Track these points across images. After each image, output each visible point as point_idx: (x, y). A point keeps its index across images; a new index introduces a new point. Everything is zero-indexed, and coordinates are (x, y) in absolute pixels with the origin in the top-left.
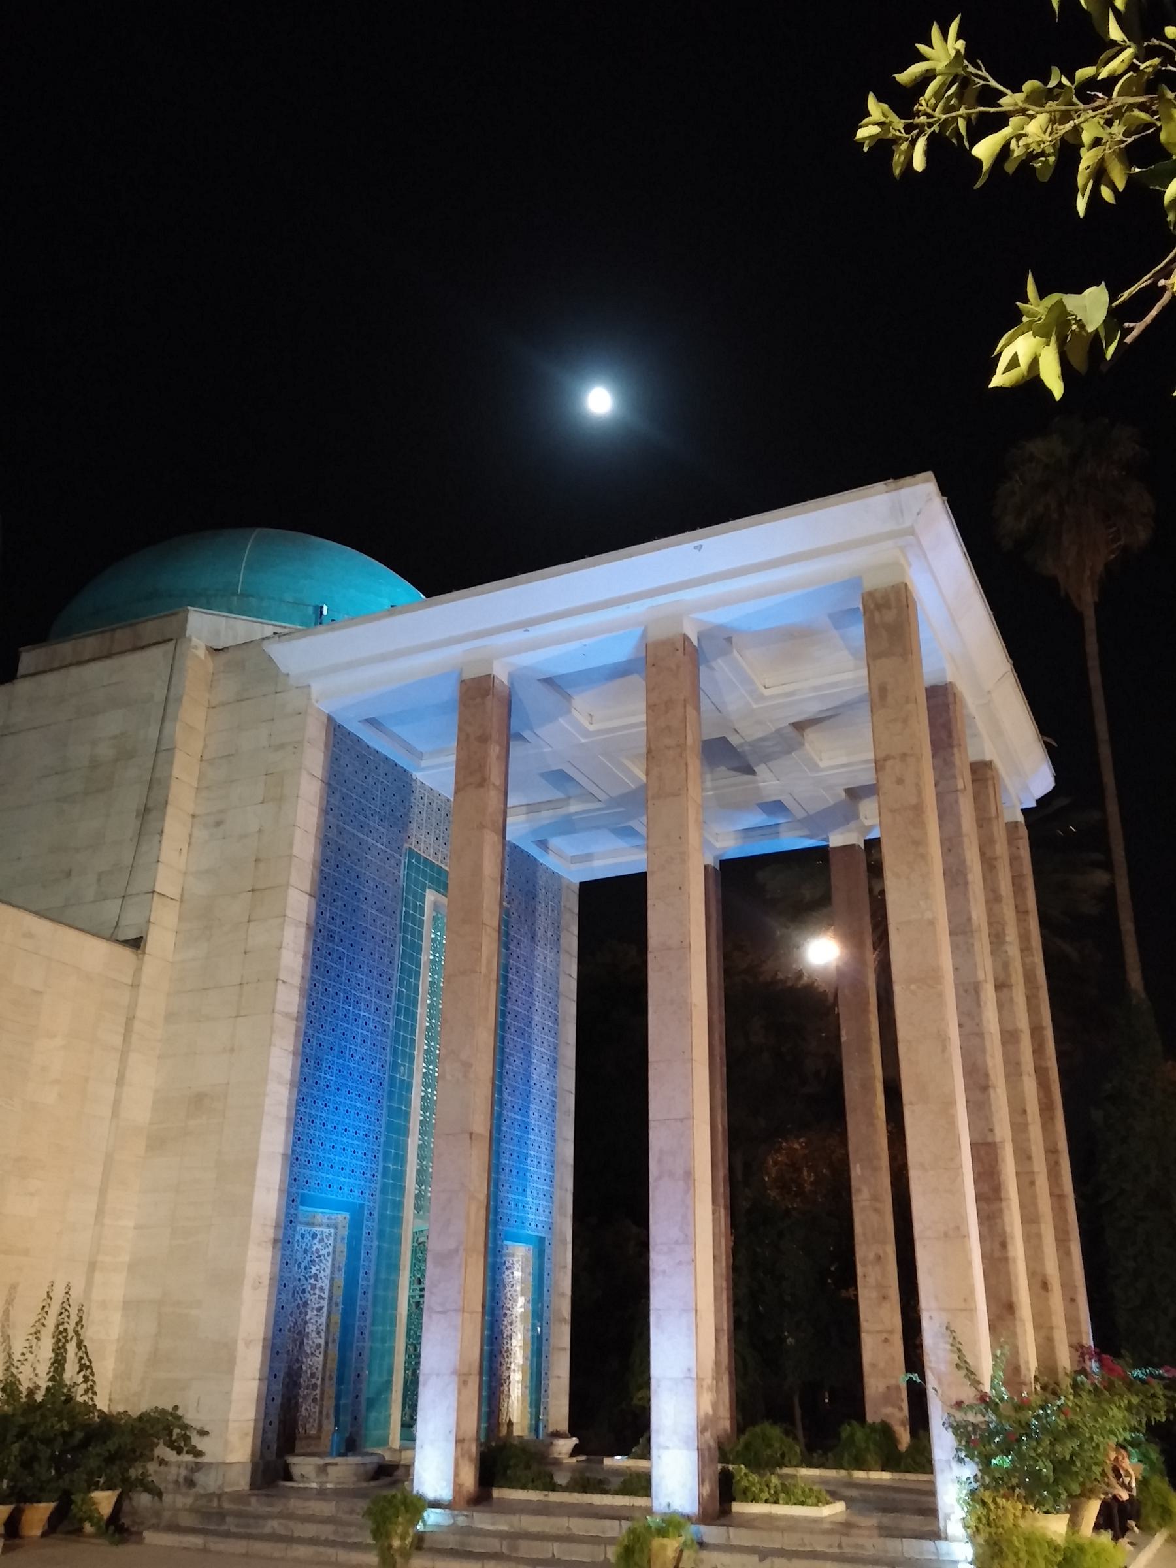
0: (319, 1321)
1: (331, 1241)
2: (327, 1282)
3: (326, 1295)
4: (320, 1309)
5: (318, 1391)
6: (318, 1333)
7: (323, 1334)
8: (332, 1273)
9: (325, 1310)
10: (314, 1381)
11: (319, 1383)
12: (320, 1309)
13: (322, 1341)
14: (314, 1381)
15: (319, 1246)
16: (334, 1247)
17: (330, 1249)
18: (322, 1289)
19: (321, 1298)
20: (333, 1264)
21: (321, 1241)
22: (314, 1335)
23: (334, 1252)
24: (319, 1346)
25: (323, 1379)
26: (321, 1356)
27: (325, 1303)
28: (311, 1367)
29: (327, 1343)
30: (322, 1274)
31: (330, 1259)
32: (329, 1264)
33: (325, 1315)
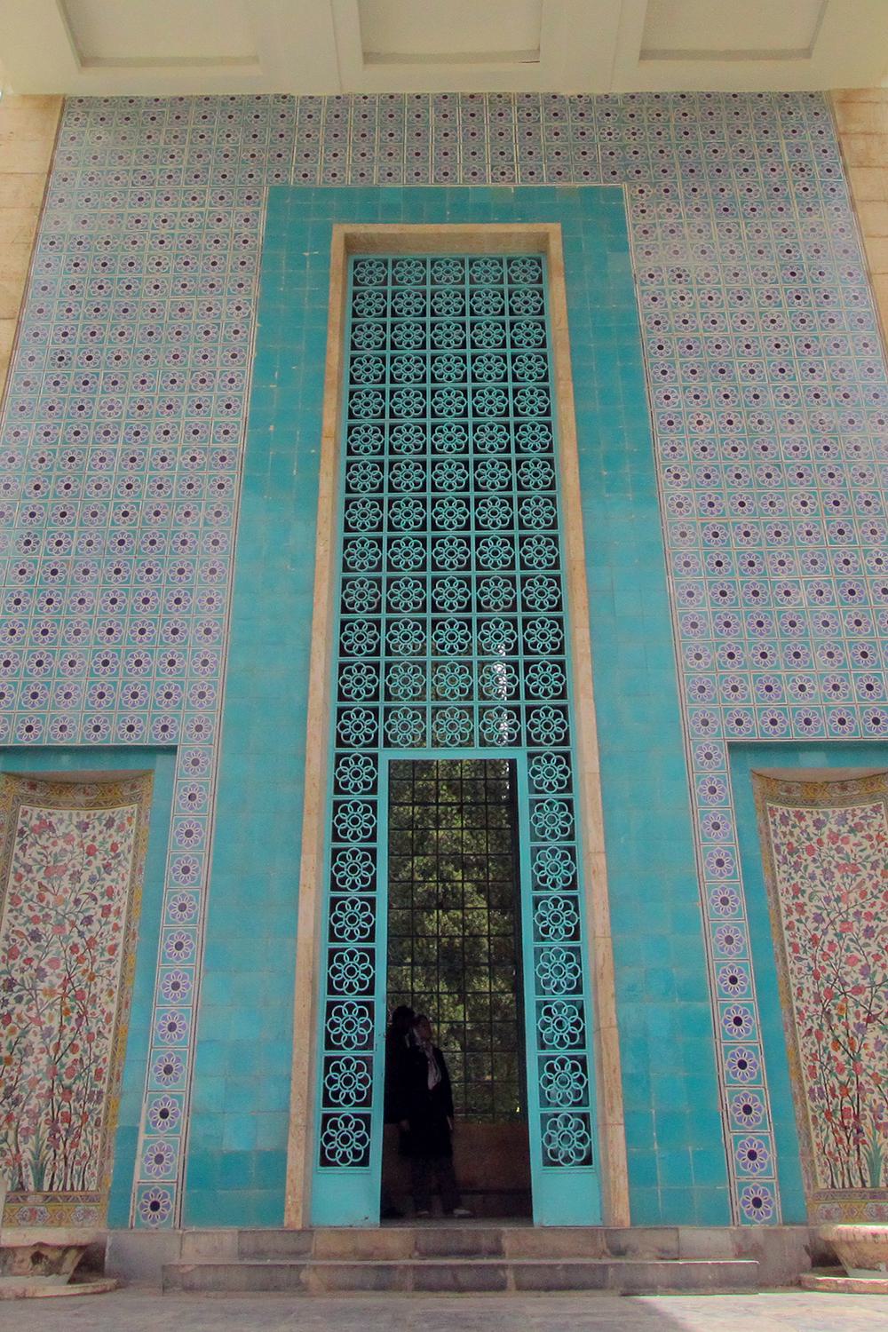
0: (113, 974)
1: (133, 827)
2: (125, 898)
3: (122, 923)
4: (112, 950)
5: (103, 1105)
6: (111, 993)
7: (116, 995)
8: (132, 881)
9: (120, 949)
11: (105, 1088)
12: (112, 950)
13: (113, 1008)
15: (117, 839)
17: (131, 841)
18: (118, 912)
19: (116, 928)
20: (134, 864)
21: (121, 828)
22: (104, 997)
23: (136, 843)
26: (111, 1036)
27: (120, 936)
28: (97, 1058)
31: (130, 857)
32: (129, 867)
33: (120, 959)
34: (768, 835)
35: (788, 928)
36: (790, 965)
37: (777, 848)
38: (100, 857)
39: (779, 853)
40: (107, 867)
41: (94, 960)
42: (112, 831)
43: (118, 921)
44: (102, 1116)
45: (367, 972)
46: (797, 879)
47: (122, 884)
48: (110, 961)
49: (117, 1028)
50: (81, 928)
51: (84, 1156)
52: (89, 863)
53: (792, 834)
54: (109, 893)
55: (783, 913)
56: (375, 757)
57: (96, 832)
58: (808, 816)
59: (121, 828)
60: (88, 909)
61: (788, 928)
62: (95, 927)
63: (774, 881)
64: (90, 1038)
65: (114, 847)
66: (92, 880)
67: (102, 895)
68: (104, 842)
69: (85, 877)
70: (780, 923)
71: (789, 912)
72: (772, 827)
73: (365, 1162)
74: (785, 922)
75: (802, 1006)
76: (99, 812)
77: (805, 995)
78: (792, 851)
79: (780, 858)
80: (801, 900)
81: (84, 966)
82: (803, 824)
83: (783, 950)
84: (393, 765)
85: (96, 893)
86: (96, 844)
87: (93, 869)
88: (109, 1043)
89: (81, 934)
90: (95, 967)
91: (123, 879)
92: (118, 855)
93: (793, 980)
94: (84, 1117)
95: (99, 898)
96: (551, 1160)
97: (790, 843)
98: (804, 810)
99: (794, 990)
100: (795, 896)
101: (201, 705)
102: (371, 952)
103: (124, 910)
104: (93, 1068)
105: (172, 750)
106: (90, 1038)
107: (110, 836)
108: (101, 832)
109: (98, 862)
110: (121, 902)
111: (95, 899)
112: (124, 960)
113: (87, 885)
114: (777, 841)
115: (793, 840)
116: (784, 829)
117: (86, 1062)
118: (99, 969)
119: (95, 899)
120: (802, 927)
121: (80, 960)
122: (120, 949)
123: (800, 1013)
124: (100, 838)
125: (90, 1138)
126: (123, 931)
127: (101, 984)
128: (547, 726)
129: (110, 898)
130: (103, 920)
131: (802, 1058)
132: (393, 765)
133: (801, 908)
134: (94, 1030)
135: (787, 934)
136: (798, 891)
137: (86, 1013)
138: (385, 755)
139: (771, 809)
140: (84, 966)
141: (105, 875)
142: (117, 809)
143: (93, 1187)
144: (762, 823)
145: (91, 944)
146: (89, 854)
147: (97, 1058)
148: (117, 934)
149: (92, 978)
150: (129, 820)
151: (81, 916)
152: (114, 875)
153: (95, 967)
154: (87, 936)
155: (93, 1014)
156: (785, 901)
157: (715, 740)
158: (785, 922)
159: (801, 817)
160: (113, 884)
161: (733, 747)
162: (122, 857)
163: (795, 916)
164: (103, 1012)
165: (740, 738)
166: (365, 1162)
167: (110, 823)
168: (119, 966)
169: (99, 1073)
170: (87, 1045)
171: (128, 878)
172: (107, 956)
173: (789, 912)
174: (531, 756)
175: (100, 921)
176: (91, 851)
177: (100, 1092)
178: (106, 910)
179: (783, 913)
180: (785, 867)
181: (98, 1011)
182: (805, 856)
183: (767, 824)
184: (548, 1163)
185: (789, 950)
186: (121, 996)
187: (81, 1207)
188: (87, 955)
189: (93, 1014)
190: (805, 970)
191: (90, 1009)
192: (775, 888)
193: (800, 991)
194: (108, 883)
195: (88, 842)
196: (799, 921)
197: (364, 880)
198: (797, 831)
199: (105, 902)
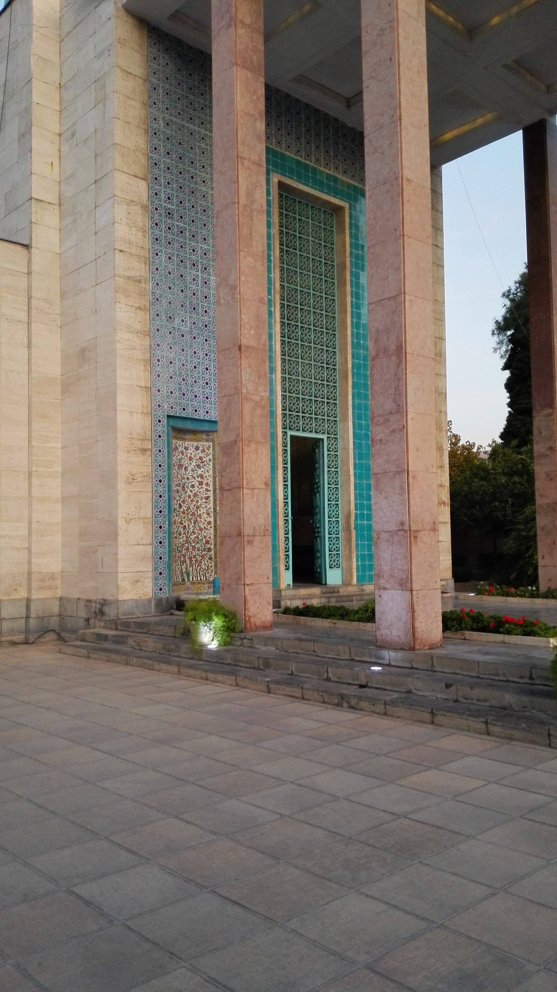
1: (211, 451)
2: (211, 479)
3: (211, 488)
4: (207, 498)
6: (208, 514)
7: (212, 515)
9: (211, 498)
10: (209, 546)
11: (212, 547)
12: (207, 498)
13: (212, 520)
14: (209, 546)
15: (201, 455)
16: (214, 455)
17: (211, 457)
18: (207, 484)
19: (207, 490)
20: (214, 467)
21: (203, 451)
22: (205, 515)
23: (214, 459)
24: (209, 523)
25: (215, 545)
26: (212, 530)
27: (211, 494)
28: (205, 537)
29: (215, 521)
31: (211, 464)
32: (211, 467)
33: (212, 502)
38: (194, 461)
40: (198, 466)
41: (197, 502)
42: (198, 451)
43: (208, 488)
44: (213, 556)
49: (215, 527)
50: (191, 489)
51: (205, 569)
52: (191, 464)
54: (201, 476)
60: (192, 482)
62: (196, 489)
66: (193, 470)
68: (195, 456)
69: (189, 469)
76: (192, 443)
81: (194, 503)
84: (291, 436)
86: (192, 456)
87: (192, 466)
89: (191, 491)
90: (199, 504)
91: (208, 472)
92: (204, 462)
94: (203, 557)
95: (196, 478)
104: (204, 540)
107: (198, 454)
108: (193, 451)
109: (194, 463)
111: (194, 478)
113: (191, 472)
117: (200, 538)
118: (201, 505)
119: (194, 478)
121: (192, 501)
124: (193, 454)
125: (207, 563)
126: (212, 492)
127: (202, 511)
130: (200, 487)
132: (291, 436)
134: (202, 527)
137: (197, 520)
140: (194, 503)
141: (198, 469)
142: (200, 443)
145: (195, 495)
148: (208, 493)
149: (198, 508)
150: (208, 449)
151: (190, 484)
152: (202, 469)
153: (199, 504)
154: (194, 492)
155: (201, 521)
160: (203, 473)
162: (205, 463)
164: (205, 520)
167: (197, 448)
169: (207, 542)
170: (200, 532)
172: (204, 500)
175: (198, 487)
178: (201, 483)
181: (203, 520)
184: (330, 567)
188: (194, 499)
189: (201, 521)
191: (198, 519)
195: (189, 455)
199: (199, 479)
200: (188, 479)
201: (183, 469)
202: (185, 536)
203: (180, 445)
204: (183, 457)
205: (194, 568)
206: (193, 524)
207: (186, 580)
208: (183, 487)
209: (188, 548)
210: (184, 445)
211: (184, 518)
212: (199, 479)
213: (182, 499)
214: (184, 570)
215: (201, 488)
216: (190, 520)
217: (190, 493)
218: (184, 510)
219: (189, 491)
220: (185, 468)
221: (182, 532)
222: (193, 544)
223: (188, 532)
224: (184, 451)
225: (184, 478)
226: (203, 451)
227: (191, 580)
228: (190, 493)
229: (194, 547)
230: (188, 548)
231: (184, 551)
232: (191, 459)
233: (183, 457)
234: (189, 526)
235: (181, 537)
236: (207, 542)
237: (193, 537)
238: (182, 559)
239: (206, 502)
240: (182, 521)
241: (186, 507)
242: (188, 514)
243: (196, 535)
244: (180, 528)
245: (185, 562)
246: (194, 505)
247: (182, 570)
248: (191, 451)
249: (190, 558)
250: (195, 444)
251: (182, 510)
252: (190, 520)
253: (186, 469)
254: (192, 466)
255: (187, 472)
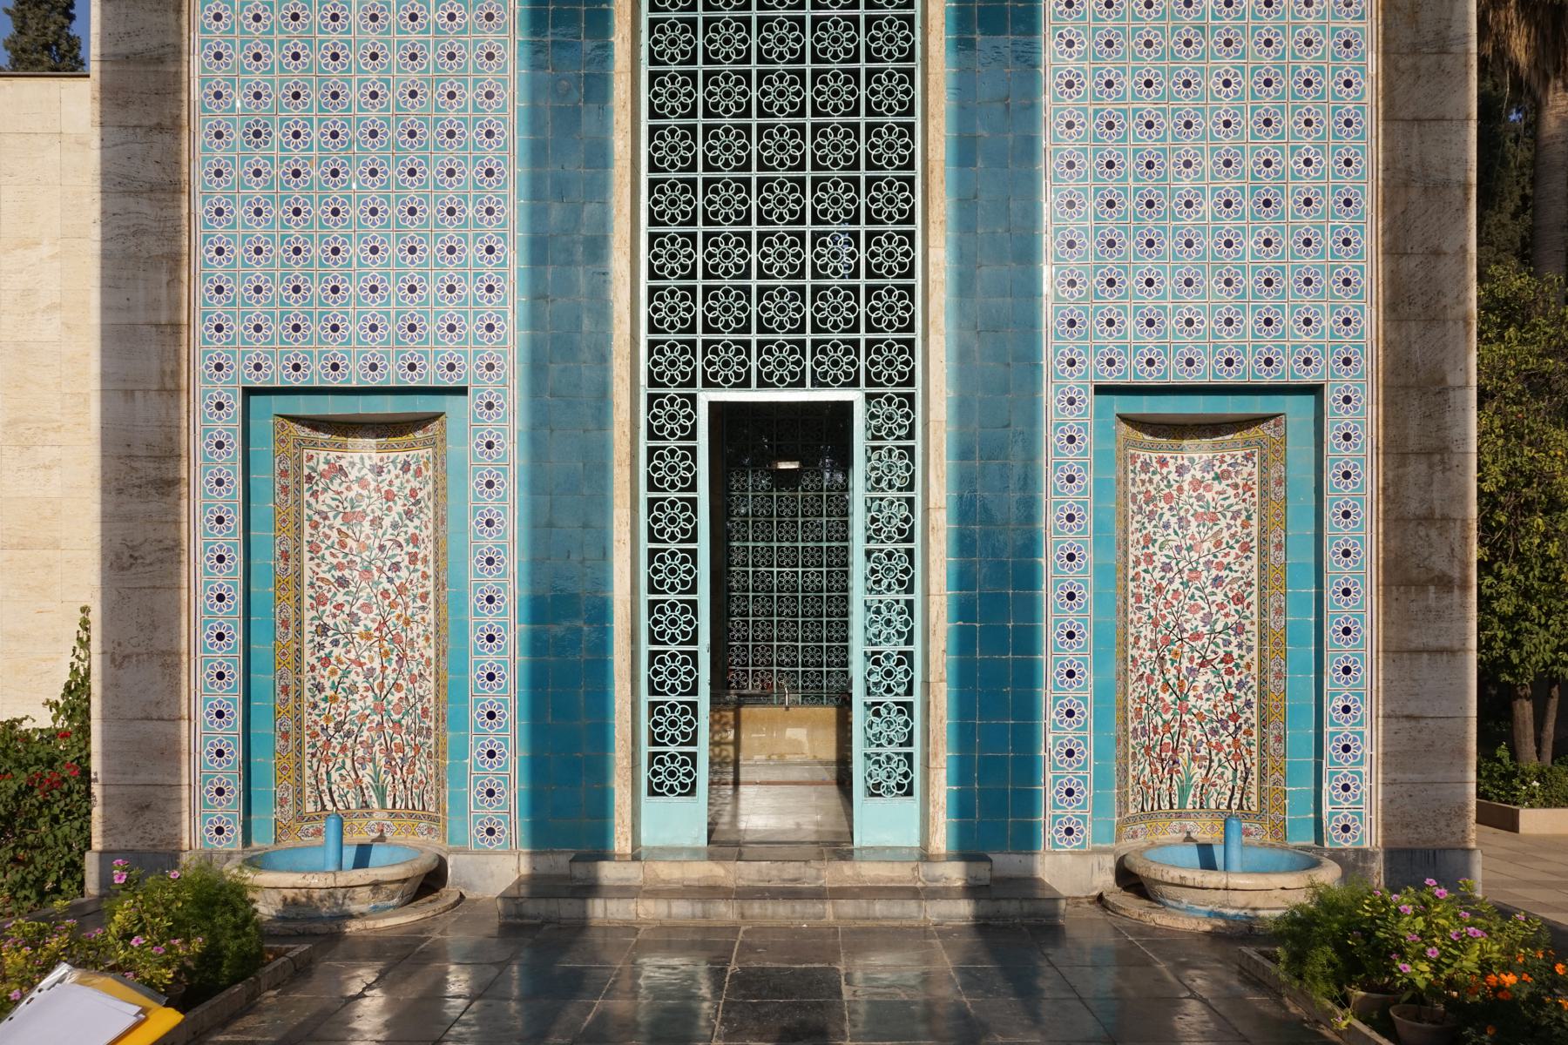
0: (427, 618)
1: (430, 472)
2: (431, 546)
3: (430, 572)
4: (424, 597)
6: (427, 639)
7: (432, 641)
8: (436, 530)
9: (431, 597)
11: (432, 725)
12: (424, 597)
13: (430, 653)
15: (415, 484)
17: (430, 488)
18: (425, 561)
19: (425, 576)
22: (421, 642)
26: (432, 679)
28: (421, 698)
30: (425, 533)
31: (431, 504)
32: (431, 515)
34: (1125, 484)
35: (1133, 580)
36: (1131, 616)
37: (1134, 497)
39: (1134, 502)
40: (408, 513)
42: (410, 475)
45: (690, 623)
46: (1150, 528)
47: (425, 533)
48: (423, 608)
53: (1151, 481)
54: (414, 540)
55: (1131, 564)
56: (693, 398)
57: (392, 476)
58: (1172, 461)
59: (418, 473)
61: (1133, 580)
62: (404, 573)
63: (1126, 531)
64: (413, 680)
65: (413, 493)
66: (395, 526)
67: (407, 541)
68: (401, 488)
69: (387, 522)
70: (1126, 575)
71: (1137, 563)
72: (1131, 475)
73: (692, 792)
74: (1131, 573)
75: (1136, 653)
76: (393, 455)
77: (1142, 643)
78: (1149, 500)
79: (1135, 508)
80: (1152, 549)
81: (398, 612)
82: (1165, 471)
83: (1126, 603)
85: (401, 539)
86: (394, 489)
88: (431, 684)
89: (390, 580)
90: (409, 613)
92: (418, 502)
93: (1131, 630)
94: (417, 748)
96: (874, 791)
97: (1148, 491)
98: (1167, 456)
99: (1131, 639)
100: (1146, 547)
101: (490, 340)
102: (694, 604)
103: (431, 558)
105: (462, 391)
106: (413, 680)
109: (398, 507)
110: (426, 550)
111: (400, 546)
112: (437, 609)
113: (390, 531)
114: (1134, 490)
115: (1151, 488)
116: (1143, 476)
117: (412, 701)
119: (400, 546)
120: (1148, 577)
121: (393, 605)
122: (431, 597)
123: (1134, 660)
124: (397, 482)
128: (890, 363)
129: (415, 546)
131: (1130, 702)
133: (1149, 558)
134: (416, 672)
135: (1131, 585)
136: (1149, 541)
137: (405, 655)
138: (705, 397)
139: (1132, 456)
140: (398, 612)
143: (432, 809)
144: (1121, 474)
145: (401, 590)
146: (388, 500)
147: (421, 698)
149: (407, 622)
150: (426, 464)
151: (388, 563)
152: (417, 522)
153: (409, 613)
156: (1133, 552)
157: (1080, 383)
158: (1131, 573)
159: (1163, 463)
161: (1100, 390)
163: (1143, 566)
165: (1109, 381)
166: (692, 792)
168: (432, 613)
169: (425, 711)
171: (431, 526)
172: (419, 603)
173: (1137, 563)
174: (869, 397)
176: (389, 496)
177: (429, 729)
178: (413, 558)
179: (1131, 564)
180: (1139, 517)
181: (417, 655)
182: (1162, 504)
183: (1126, 473)
185: (1131, 600)
186: (437, 643)
187: (424, 824)
188: (399, 600)
190: (1144, 619)
192: (1126, 540)
193: (1137, 639)
194: (411, 530)
196: (1146, 571)
197: (684, 532)
198: (1157, 478)
199: (410, 548)
200: (382, 548)
201: (366, 523)
202: (370, 694)
203: (353, 464)
204: (365, 493)
205: (398, 777)
206: (394, 665)
207: (376, 806)
208: (367, 570)
209: (381, 724)
210: (368, 463)
211: (370, 648)
212: (410, 548)
213: (361, 601)
214: (367, 780)
215: (415, 571)
216: (387, 654)
217: (388, 586)
218: (367, 629)
219: (384, 580)
220: (372, 521)
221: (361, 685)
222: (396, 717)
223: (382, 686)
224: (370, 477)
225: (368, 548)
226: (418, 473)
227: (389, 805)
228: (388, 586)
229: (397, 724)
230: (381, 724)
231: (366, 734)
232: (389, 496)
233: (365, 493)
234: (384, 668)
235: (356, 697)
236: (425, 711)
237: (395, 697)
238: (360, 753)
239: (423, 608)
240: (358, 656)
241: (373, 621)
242: (381, 639)
243: (402, 694)
244: (353, 676)
245: (372, 760)
246: (399, 617)
247: (358, 779)
248: (389, 477)
249: (388, 751)
250: (402, 456)
251: (361, 629)
252: (387, 654)
253: (376, 522)
254: (394, 516)
255: (380, 532)
